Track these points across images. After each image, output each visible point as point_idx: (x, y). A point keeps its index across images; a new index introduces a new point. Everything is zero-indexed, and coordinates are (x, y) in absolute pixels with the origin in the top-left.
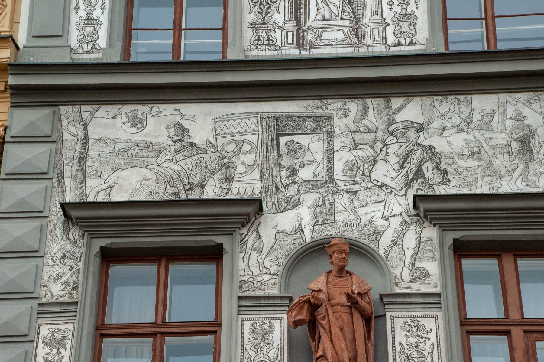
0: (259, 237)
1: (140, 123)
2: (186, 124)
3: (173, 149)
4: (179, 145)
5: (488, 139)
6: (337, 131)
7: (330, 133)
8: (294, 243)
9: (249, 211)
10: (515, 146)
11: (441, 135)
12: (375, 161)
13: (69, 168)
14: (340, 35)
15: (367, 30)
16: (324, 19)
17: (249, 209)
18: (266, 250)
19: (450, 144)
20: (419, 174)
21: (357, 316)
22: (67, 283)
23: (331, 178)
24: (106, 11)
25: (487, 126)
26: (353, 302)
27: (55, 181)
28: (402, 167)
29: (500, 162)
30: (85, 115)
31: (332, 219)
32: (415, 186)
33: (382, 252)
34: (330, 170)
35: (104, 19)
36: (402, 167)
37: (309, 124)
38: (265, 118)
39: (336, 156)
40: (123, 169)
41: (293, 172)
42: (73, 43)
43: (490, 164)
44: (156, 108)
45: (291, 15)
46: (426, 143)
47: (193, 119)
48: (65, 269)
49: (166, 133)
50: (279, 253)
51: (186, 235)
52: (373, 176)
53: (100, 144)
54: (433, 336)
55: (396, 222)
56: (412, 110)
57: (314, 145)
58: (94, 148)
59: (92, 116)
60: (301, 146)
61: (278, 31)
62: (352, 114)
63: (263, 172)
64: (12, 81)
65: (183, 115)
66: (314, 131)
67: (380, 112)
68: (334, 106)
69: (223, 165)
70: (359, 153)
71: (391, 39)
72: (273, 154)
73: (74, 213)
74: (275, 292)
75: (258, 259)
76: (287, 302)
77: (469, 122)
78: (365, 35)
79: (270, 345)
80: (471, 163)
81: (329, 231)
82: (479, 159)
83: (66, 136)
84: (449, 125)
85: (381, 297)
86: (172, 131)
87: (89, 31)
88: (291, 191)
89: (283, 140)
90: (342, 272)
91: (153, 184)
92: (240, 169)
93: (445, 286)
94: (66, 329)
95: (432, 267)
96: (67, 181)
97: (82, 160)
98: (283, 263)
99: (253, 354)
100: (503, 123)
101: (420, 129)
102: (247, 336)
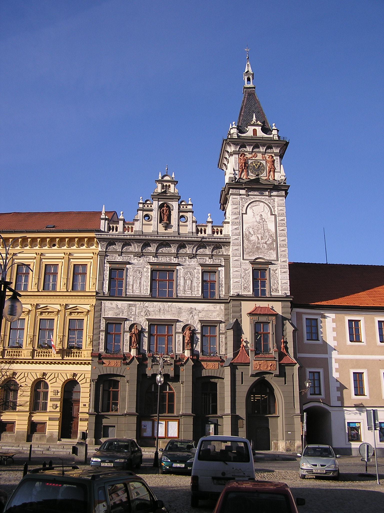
1: (112, 304)
9: (126, 320)
56: (147, 304)
57: (134, 308)
68: (137, 303)
97: (105, 309)
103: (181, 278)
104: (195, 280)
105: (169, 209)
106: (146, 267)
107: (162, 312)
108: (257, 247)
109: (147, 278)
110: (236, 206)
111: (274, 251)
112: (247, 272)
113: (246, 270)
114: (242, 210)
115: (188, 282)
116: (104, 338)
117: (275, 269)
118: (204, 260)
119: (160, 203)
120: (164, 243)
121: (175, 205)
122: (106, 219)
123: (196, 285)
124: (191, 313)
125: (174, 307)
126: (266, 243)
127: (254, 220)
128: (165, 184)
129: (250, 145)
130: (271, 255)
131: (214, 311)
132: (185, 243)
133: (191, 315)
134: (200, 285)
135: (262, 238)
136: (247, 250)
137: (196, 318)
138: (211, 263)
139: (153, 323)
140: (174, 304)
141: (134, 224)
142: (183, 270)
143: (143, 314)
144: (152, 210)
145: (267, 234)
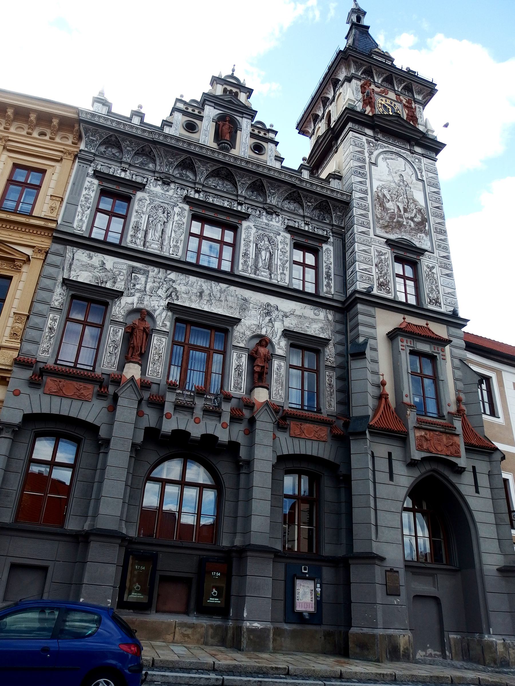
1: (91, 257)
2: (105, 262)
3: (99, 268)
8: (130, 307)
9: (119, 294)
10: (198, 294)
13: (66, 266)
14: (157, 246)
17: (119, 294)
18: (122, 307)
20: (170, 295)
21: (145, 334)
22: (60, 302)
24: (87, 219)
25: (192, 286)
26: (144, 330)
29: (193, 297)
30: (74, 251)
32: (169, 298)
33: (155, 316)
34: (145, 287)
35: (86, 221)
37: (142, 271)
38: (130, 266)
41: (134, 285)
42: (75, 226)
43: (191, 297)
44: (97, 254)
45: (143, 236)
47: (107, 261)
50: (126, 309)
53: (77, 261)
54: (164, 344)
55: (161, 308)
56: (173, 275)
57: (142, 278)
64: (54, 234)
66: (143, 274)
67: (163, 273)
68: (151, 268)
70: (154, 284)
71: (171, 252)
73: (66, 282)
74: (122, 321)
75: (119, 309)
79: (117, 336)
80: (185, 296)
81: (141, 306)
83: (67, 256)
85: (152, 329)
86: (100, 263)
87: (81, 224)
88: (133, 291)
89: (133, 274)
91: (91, 278)
92: (119, 280)
93: (170, 330)
94: (58, 317)
95: (168, 324)
96: (65, 270)
97: (71, 265)
101: (174, 282)
102: (111, 332)
103: (251, 244)
104: (278, 254)
105: (235, 127)
106: (181, 205)
107: (205, 297)
108: (398, 222)
109: (179, 225)
111: (426, 235)
112: (383, 257)
113: (380, 254)
114: (370, 159)
117: (431, 265)
121: (245, 124)
123: (279, 263)
124: (268, 314)
125: (233, 293)
126: (412, 219)
127: (390, 178)
128: (229, 88)
129: (380, 74)
130: (423, 241)
131: (314, 321)
133: (268, 318)
135: (405, 210)
136: (381, 222)
137: (279, 327)
140: (232, 288)
142: (254, 230)
145: (412, 206)
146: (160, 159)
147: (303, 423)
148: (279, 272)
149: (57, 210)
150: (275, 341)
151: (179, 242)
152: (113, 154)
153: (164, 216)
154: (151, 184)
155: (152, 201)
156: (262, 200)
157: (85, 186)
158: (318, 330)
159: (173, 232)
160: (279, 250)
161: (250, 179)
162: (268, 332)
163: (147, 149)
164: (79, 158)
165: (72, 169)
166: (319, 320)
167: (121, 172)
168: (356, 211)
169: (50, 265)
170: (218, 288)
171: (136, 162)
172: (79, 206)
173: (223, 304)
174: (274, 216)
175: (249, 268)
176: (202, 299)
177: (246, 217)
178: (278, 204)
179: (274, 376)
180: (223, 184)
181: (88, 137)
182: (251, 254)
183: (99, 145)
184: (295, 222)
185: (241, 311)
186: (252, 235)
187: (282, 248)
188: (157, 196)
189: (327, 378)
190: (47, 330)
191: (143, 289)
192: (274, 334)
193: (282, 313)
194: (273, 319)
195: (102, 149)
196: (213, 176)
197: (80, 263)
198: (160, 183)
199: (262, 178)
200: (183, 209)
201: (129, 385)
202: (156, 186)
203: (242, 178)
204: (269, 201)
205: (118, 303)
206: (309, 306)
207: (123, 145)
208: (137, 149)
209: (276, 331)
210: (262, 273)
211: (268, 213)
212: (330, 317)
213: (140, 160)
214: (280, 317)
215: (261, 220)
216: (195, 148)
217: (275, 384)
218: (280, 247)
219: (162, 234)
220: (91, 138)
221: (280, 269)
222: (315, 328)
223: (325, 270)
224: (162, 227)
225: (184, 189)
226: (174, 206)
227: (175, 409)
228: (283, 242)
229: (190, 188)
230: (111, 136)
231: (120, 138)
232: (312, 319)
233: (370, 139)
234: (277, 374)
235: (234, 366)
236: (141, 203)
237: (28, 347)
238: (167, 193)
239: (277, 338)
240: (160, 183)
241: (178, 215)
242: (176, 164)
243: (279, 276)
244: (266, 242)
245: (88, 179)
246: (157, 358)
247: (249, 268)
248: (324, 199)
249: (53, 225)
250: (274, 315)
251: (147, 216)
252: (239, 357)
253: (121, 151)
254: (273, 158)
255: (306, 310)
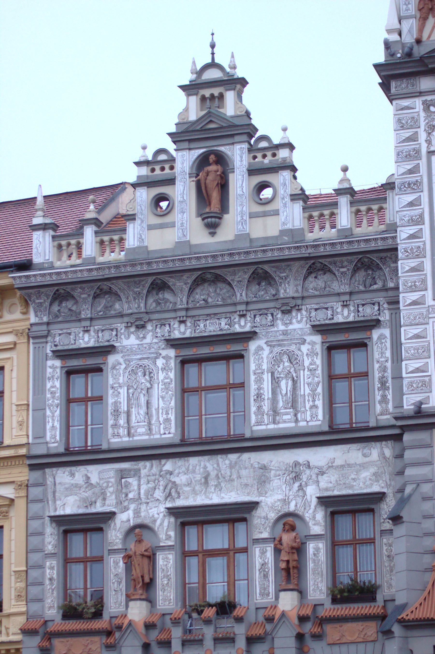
0: (115, 524)
1: (72, 475)
2: (89, 475)
3: (85, 486)
4: (87, 484)
5: (194, 478)
6: (142, 476)
7: (140, 477)
8: (127, 526)
9: (111, 515)
10: (203, 480)
11: (178, 476)
12: (155, 489)
13: (50, 497)
15: (154, 427)
16: (138, 422)
19: (181, 480)
20: (170, 494)
23: (140, 498)
25: (194, 472)
27: (46, 502)
28: (164, 491)
29: (197, 488)
31: (140, 515)
33: (156, 529)
34: (139, 494)
35: (58, 426)
36: (164, 491)
37: (132, 473)
39: (142, 487)
40: (68, 496)
41: (127, 495)
42: (48, 439)
45: (126, 421)
46: (173, 480)
47: (91, 473)
48: (52, 539)
49: (82, 480)
51: (91, 524)
52: (155, 495)
54: (171, 561)
55: (161, 515)
56: (168, 465)
58: (58, 487)
59: (56, 472)
60: (130, 483)
61: (121, 428)
62: (148, 468)
63: (116, 496)
65: (88, 471)
66: (134, 476)
67: (157, 466)
68: (141, 464)
69: (102, 493)
70: (149, 485)
71: (162, 432)
72: (120, 487)
75: (115, 535)
76: (124, 551)
77: (188, 469)
78: (152, 429)
79: (119, 567)
80: (187, 489)
81: (139, 521)
82: (190, 487)
83: (48, 483)
84: (181, 471)
87: (53, 433)
88: (126, 504)
89: (123, 480)
90: (140, 541)
92: (108, 494)
95: (172, 534)
96: (50, 502)
97: (54, 492)
98: (123, 534)
99: (113, 570)
100: (199, 470)
101: (171, 473)
102: (112, 564)
103: (265, 376)
104: (304, 376)
106: (164, 353)
107: (212, 482)
110: (407, 133)
115: (285, 386)
116: (55, 576)
118: (330, 312)
119: (197, 153)
120: (209, 275)
121: (238, 155)
122: (44, 227)
123: (308, 391)
124: (297, 478)
125: (247, 464)
128: (207, 93)
131: (363, 466)
132: (266, 267)
133: (297, 485)
134: (320, 390)
137: (312, 492)
138: (351, 319)
139: (189, 518)
140: (246, 456)
141: (124, 230)
142: (267, 350)
143: (159, 494)
144: (171, 181)
146: (124, 294)
147: (343, 624)
148: (307, 408)
149: (25, 424)
150: (307, 516)
151: (170, 413)
152: (70, 310)
153: (146, 380)
154: (123, 337)
155: (128, 361)
156: (274, 293)
157: (48, 375)
158: (370, 479)
159: (160, 399)
160: (306, 370)
161: (245, 273)
162: (298, 506)
163: (105, 287)
164: (34, 338)
165: (28, 352)
166: (372, 463)
167: (83, 335)
168: (404, 265)
169: (33, 501)
170: (227, 462)
171: (99, 309)
172: (47, 408)
173: (235, 483)
174: (294, 313)
175: (265, 417)
176: (208, 486)
177: (251, 336)
178: (297, 291)
179: (310, 565)
180: (216, 291)
181: (34, 301)
182: (266, 393)
183: (51, 305)
184: (327, 309)
185: (259, 486)
186: (265, 361)
187: (311, 364)
188: (131, 351)
189: (385, 548)
190: (47, 582)
191: (137, 497)
192: (307, 504)
193: (316, 471)
194: (303, 483)
195: (55, 308)
196: (198, 285)
197: (63, 487)
198: (133, 329)
199: (260, 266)
200: (167, 358)
201: (129, 631)
202: (129, 338)
203: (235, 275)
204: (282, 291)
205: (113, 525)
206: (354, 446)
207: (75, 294)
208: (92, 293)
209: (309, 500)
210: (285, 417)
211: (283, 312)
212: (388, 452)
213: (103, 302)
214: (314, 477)
215: (276, 329)
216: (158, 266)
217: (311, 577)
218: (307, 363)
219: (148, 408)
220: (37, 301)
221: (309, 401)
222: (365, 478)
223: (377, 375)
224: (146, 398)
225: (165, 325)
226: (157, 358)
227: (183, 645)
228: (312, 353)
229: (172, 320)
230: (58, 290)
231: (68, 288)
232: (360, 465)
233: (429, 98)
234: (314, 561)
235: (258, 566)
236: (115, 372)
237: (35, 607)
238: (145, 341)
239: (311, 511)
240: (133, 329)
241: (163, 369)
242: (145, 292)
243: (308, 413)
244: (287, 364)
245: (50, 363)
246: (166, 582)
247: (265, 417)
248: (361, 256)
249: (23, 451)
250: (304, 478)
251: (126, 388)
252: (263, 553)
253: (76, 302)
254: (288, 199)
255: (350, 454)
